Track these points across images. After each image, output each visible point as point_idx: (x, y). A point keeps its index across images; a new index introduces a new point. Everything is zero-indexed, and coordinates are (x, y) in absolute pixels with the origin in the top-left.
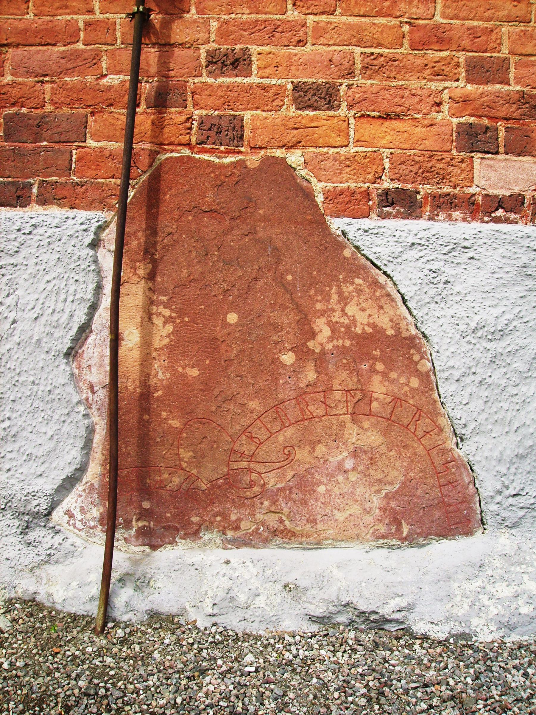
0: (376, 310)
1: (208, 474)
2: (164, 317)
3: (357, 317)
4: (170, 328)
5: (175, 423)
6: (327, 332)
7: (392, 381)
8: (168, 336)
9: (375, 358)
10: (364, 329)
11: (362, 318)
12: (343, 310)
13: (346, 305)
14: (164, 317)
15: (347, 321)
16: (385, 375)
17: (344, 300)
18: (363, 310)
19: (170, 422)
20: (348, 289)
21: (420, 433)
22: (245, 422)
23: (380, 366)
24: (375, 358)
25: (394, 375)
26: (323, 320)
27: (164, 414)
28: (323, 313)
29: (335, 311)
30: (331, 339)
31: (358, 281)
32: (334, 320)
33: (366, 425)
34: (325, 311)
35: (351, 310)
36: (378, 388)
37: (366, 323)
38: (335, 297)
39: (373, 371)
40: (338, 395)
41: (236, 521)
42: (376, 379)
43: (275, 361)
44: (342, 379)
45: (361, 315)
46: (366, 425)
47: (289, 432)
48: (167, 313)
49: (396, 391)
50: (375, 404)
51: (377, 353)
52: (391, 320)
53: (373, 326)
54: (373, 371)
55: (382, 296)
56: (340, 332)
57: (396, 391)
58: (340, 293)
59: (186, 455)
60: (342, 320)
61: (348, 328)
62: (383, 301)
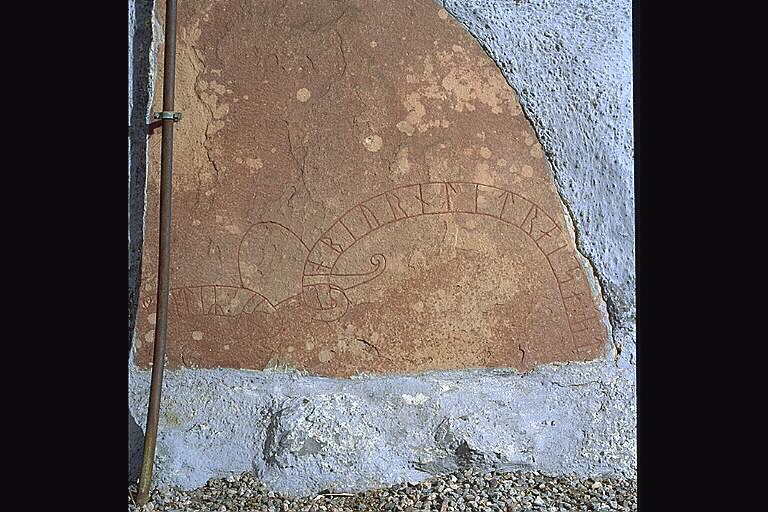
0: (479, 84)
1: (281, 290)
2: (217, 95)
3: (457, 92)
4: (225, 108)
5: (234, 229)
6: (421, 110)
7: (499, 171)
8: (223, 119)
9: (479, 142)
10: (465, 106)
11: (462, 93)
12: (440, 84)
13: (442, 77)
14: (217, 95)
15: (444, 97)
16: (492, 162)
17: (441, 72)
18: (464, 83)
19: (227, 227)
20: (445, 57)
21: (535, 235)
22: (324, 225)
23: (485, 152)
24: (479, 142)
25: (501, 163)
26: (415, 96)
27: (219, 218)
28: (415, 88)
29: (429, 85)
30: (425, 119)
31: (456, 48)
32: (429, 95)
33: (471, 224)
34: (418, 85)
35: (449, 83)
36: (484, 177)
37: (467, 99)
38: (430, 68)
39: (477, 158)
40: (437, 188)
41: (312, 351)
42: (482, 168)
43: (359, 148)
44: (440, 168)
45: (462, 88)
46: (471, 224)
47: (378, 236)
48: (220, 89)
49: (506, 182)
50: (481, 199)
51: (481, 135)
52: (498, 96)
53: (477, 103)
54: (477, 158)
55: (486, 66)
56: (436, 110)
57: (506, 182)
58: (435, 62)
59: (248, 269)
60: (438, 96)
61: (445, 105)
62: (487, 71)
